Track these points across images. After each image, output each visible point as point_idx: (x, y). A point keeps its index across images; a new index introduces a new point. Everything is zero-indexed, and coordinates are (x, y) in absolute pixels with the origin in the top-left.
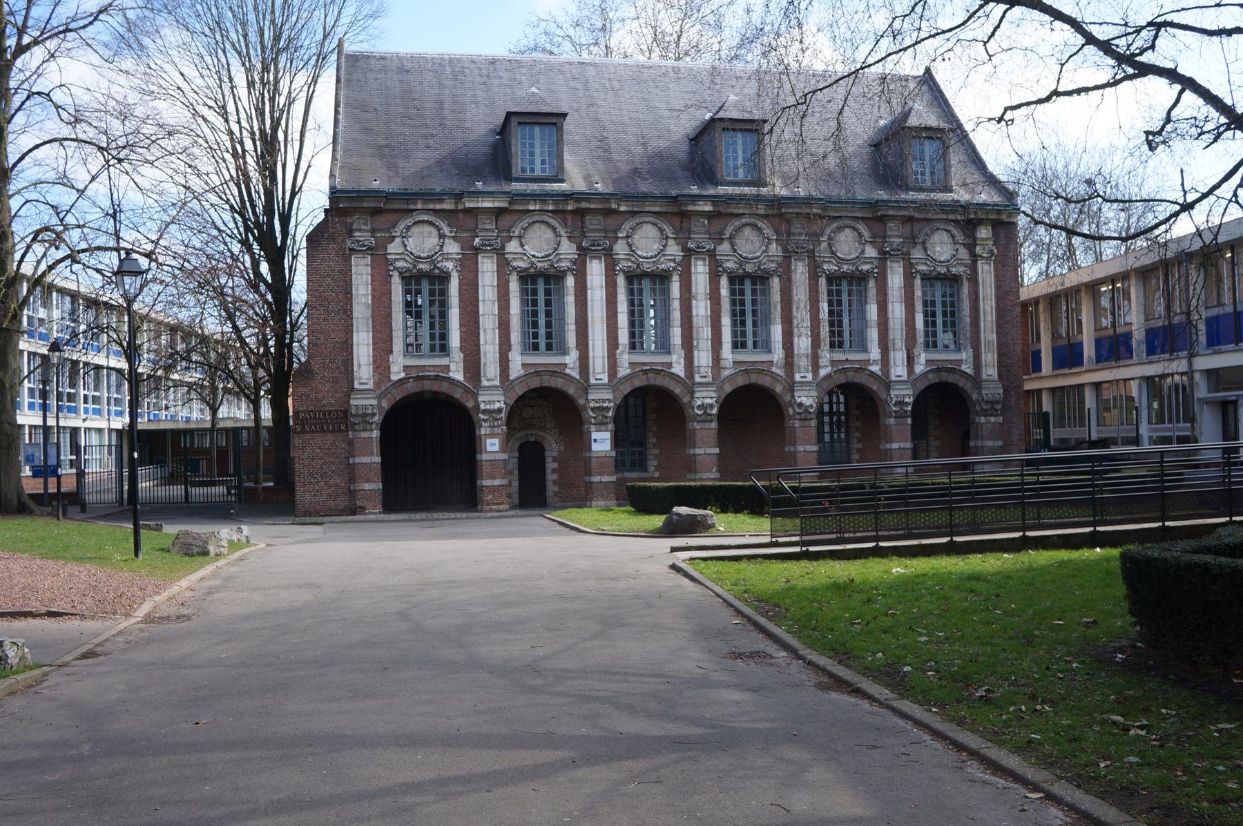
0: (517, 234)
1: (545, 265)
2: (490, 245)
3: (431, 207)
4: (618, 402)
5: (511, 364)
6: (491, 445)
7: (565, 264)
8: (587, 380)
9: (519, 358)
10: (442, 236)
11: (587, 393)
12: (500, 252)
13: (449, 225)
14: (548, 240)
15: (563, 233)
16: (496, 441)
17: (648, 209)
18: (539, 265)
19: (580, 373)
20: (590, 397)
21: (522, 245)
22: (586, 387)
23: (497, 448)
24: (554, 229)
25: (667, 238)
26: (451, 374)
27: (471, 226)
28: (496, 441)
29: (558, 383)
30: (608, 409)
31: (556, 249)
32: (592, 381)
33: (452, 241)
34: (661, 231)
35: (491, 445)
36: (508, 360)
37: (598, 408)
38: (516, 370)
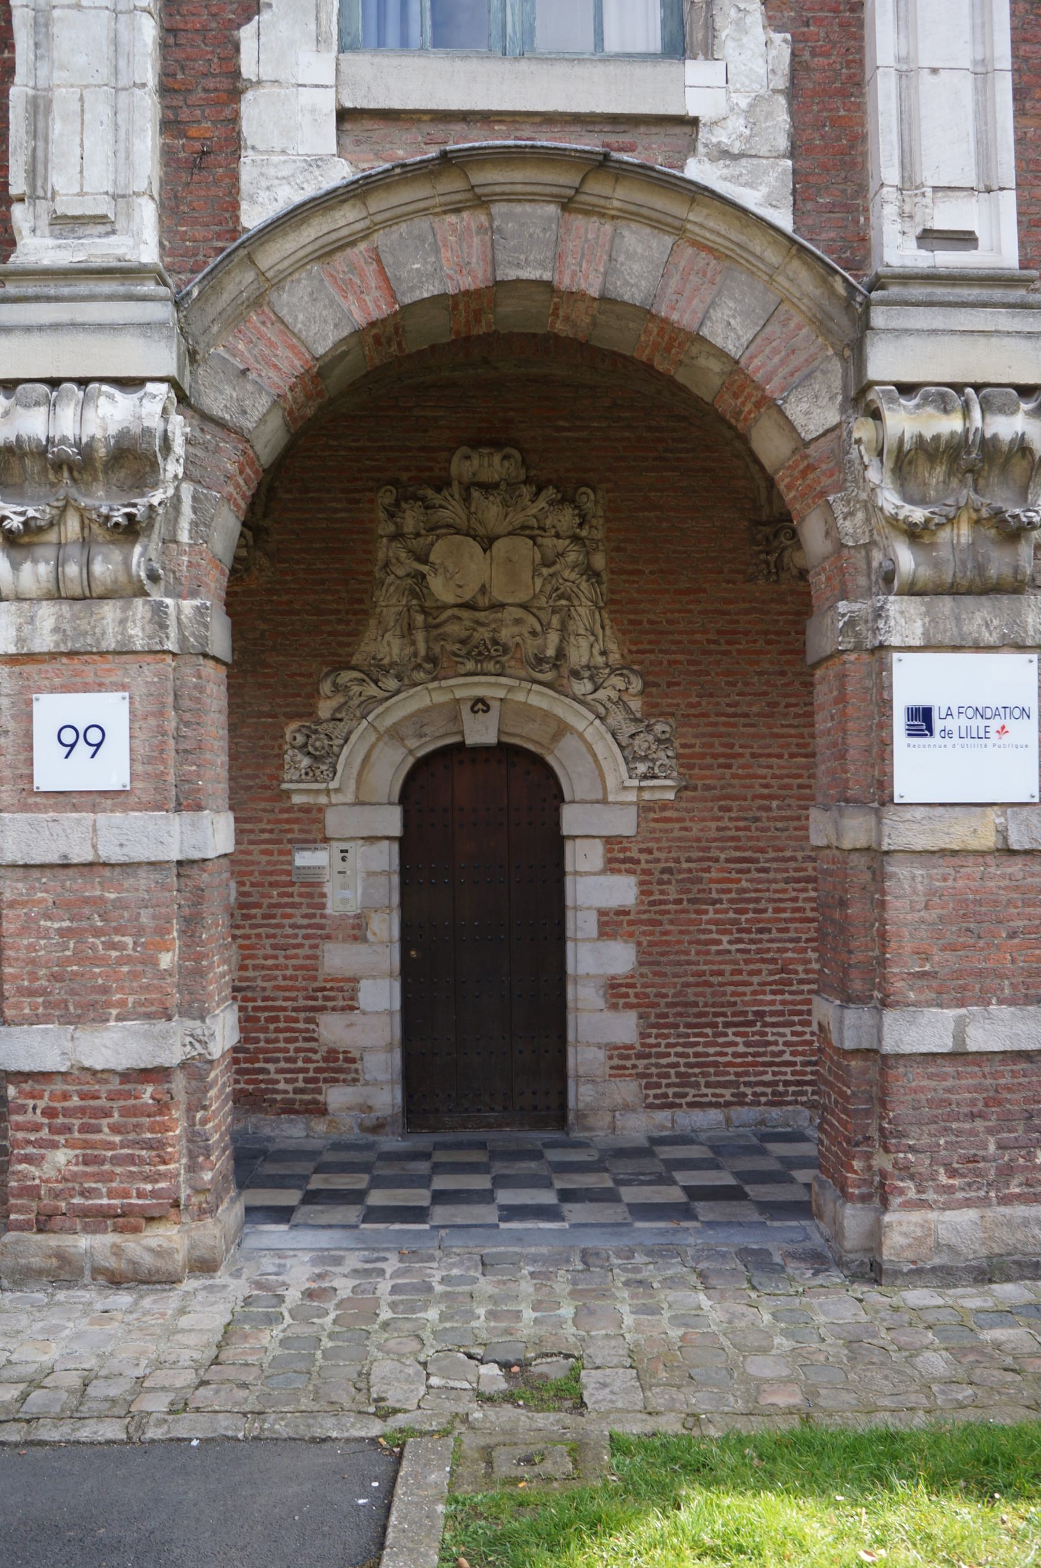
5: (255, 115)
6: (76, 739)
9: (318, 66)
11: (855, 353)
16: (110, 710)
19: (802, 191)
20: (885, 363)
22: (849, 296)
23: (112, 769)
28: (110, 710)
29: (621, 263)
32: (897, 249)
35: (76, 739)
36: (233, 87)
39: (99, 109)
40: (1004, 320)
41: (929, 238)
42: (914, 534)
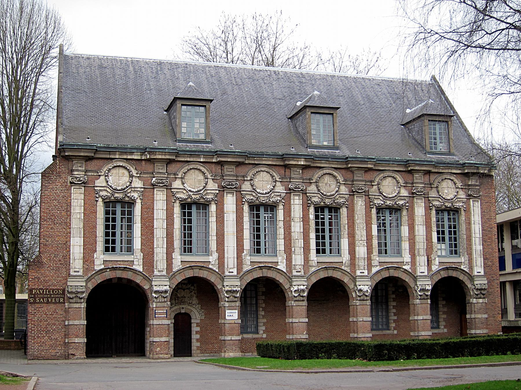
0: (180, 176)
1: (198, 197)
2: (162, 183)
3: (125, 157)
4: (243, 288)
7: (210, 197)
8: (224, 272)
10: (131, 176)
12: (168, 188)
13: (136, 169)
14: (199, 181)
15: (209, 176)
17: (264, 162)
18: (193, 196)
21: (183, 184)
24: (204, 174)
25: (276, 181)
26: (134, 267)
27: (151, 171)
29: (203, 274)
30: (236, 292)
31: (204, 187)
33: (137, 180)
34: (272, 176)
37: (230, 291)
38: (177, 265)
39: (162, 261)
40: (235, 280)
41: (229, 272)
42: (228, 298)
